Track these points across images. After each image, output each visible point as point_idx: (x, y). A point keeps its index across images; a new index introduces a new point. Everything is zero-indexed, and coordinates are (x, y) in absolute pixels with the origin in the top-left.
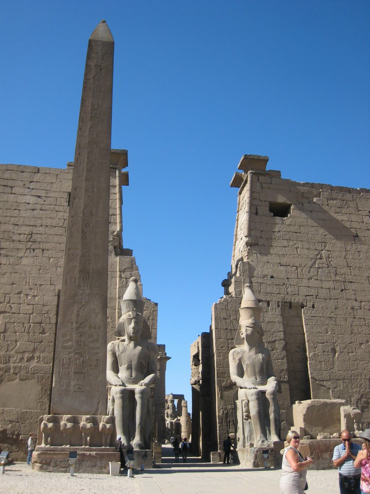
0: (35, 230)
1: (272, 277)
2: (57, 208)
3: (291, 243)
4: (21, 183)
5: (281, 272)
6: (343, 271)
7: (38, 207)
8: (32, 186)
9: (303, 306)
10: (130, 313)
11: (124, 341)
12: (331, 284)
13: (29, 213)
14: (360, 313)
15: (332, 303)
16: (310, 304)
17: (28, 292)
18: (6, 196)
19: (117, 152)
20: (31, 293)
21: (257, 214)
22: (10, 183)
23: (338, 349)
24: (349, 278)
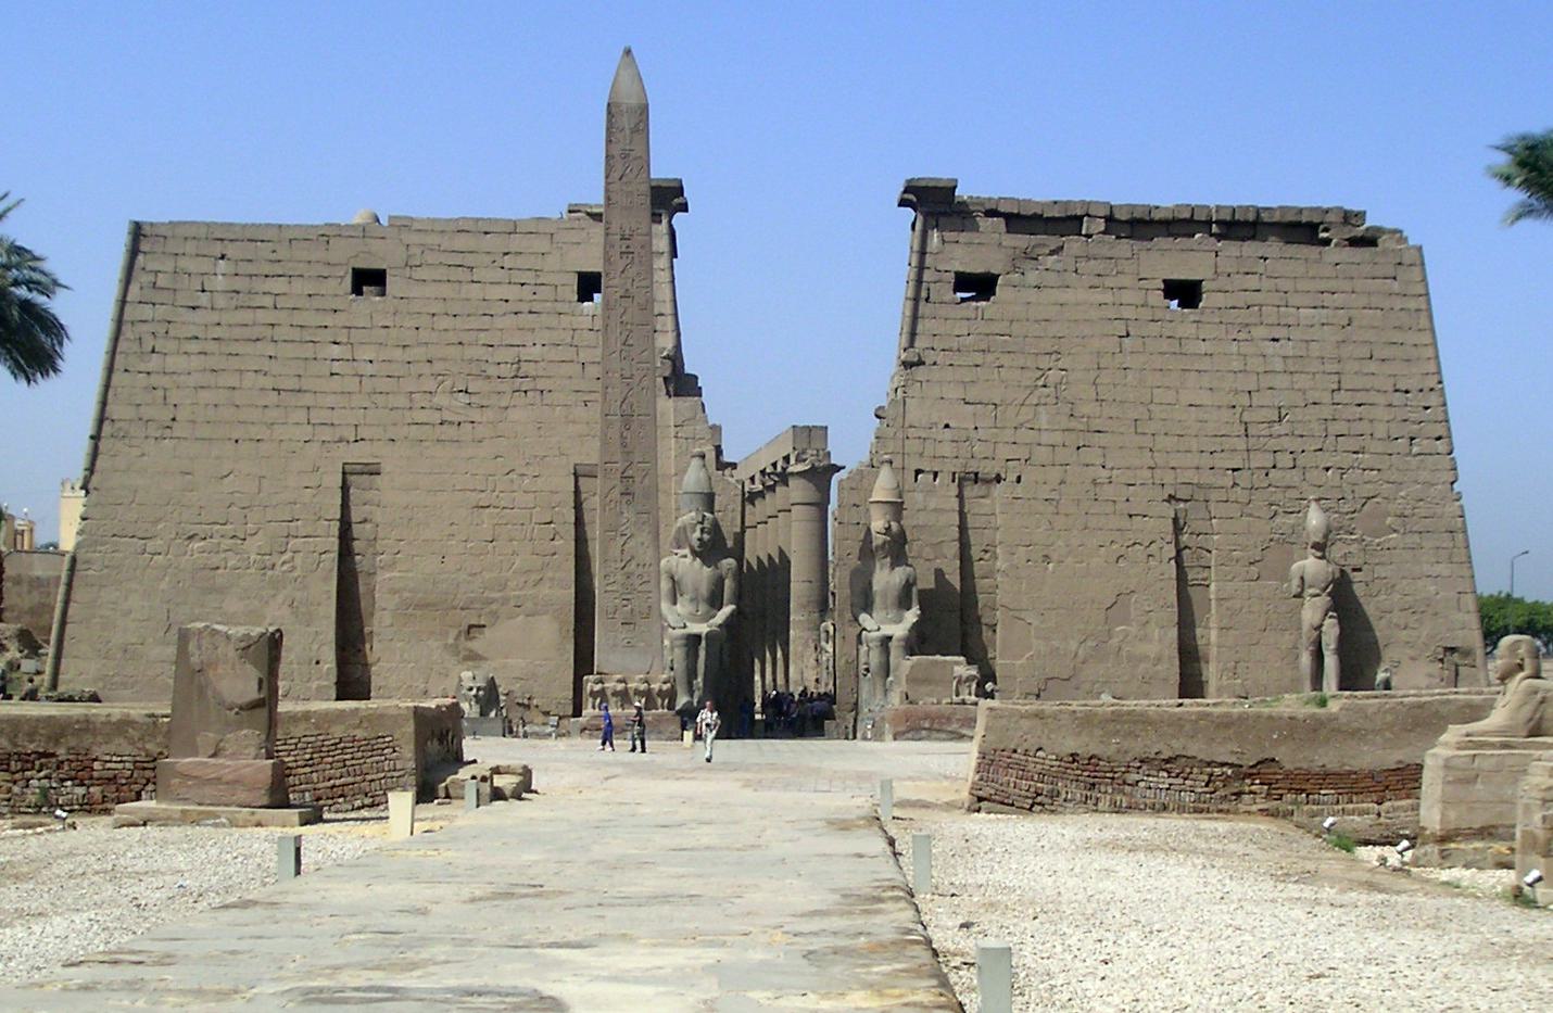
0: (525, 354)
1: (947, 426)
2: (559, 307)
3: (990, 358)
4: (487, 259)
5: (963, 418)
6: (1086, 409)
7: (525, 307)
8: (508, 261)
9: (998, 479)
10: (693, 514)
11: (685, 556)
12: (1057, 438)
13: (510, 321)
14: (1108, 492)
15: (1055, 474)
16: (1012, 477)
17: (524, 471)
18: (465, 287)
19: (664, 185)
20: (530, 471)
21: (927, 300)
22: (469, 260)
23: (1055, 556)
24: (1096, 424)
